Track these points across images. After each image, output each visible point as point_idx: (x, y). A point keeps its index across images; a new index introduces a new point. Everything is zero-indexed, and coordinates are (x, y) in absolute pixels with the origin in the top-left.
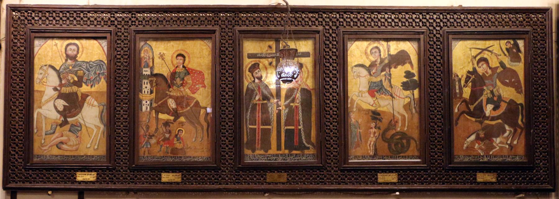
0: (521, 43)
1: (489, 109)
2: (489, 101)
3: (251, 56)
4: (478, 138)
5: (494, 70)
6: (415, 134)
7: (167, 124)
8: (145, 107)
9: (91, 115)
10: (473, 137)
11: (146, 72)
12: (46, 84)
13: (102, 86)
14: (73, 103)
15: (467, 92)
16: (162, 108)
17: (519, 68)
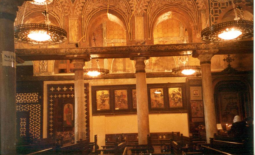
0: (181, 88)
1: (176, 99)
2: (176, 98)
3: (134, 92)
4: (174, 104)
5: (176, 93)
6: (163, 103)
7: (120, 104)
8: (116, 101)
9: (107, 103)
10: (173, 104)
11: (116, 95)
12: (98, 98)
13: (108, 98)
14: (104, 101)
15: (172, 96)
16: (119, 101)
17: (181, 92)
